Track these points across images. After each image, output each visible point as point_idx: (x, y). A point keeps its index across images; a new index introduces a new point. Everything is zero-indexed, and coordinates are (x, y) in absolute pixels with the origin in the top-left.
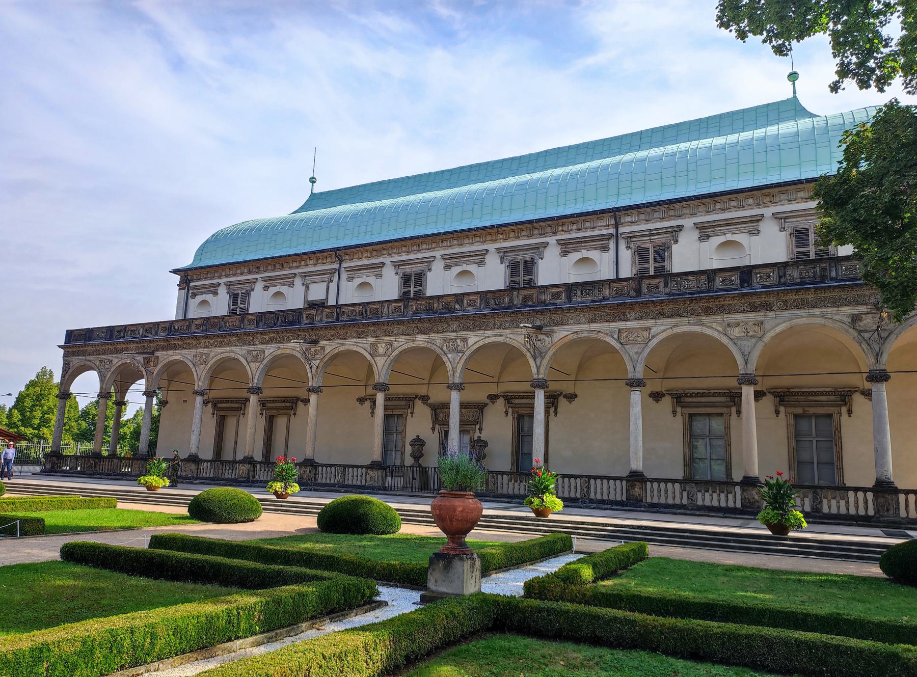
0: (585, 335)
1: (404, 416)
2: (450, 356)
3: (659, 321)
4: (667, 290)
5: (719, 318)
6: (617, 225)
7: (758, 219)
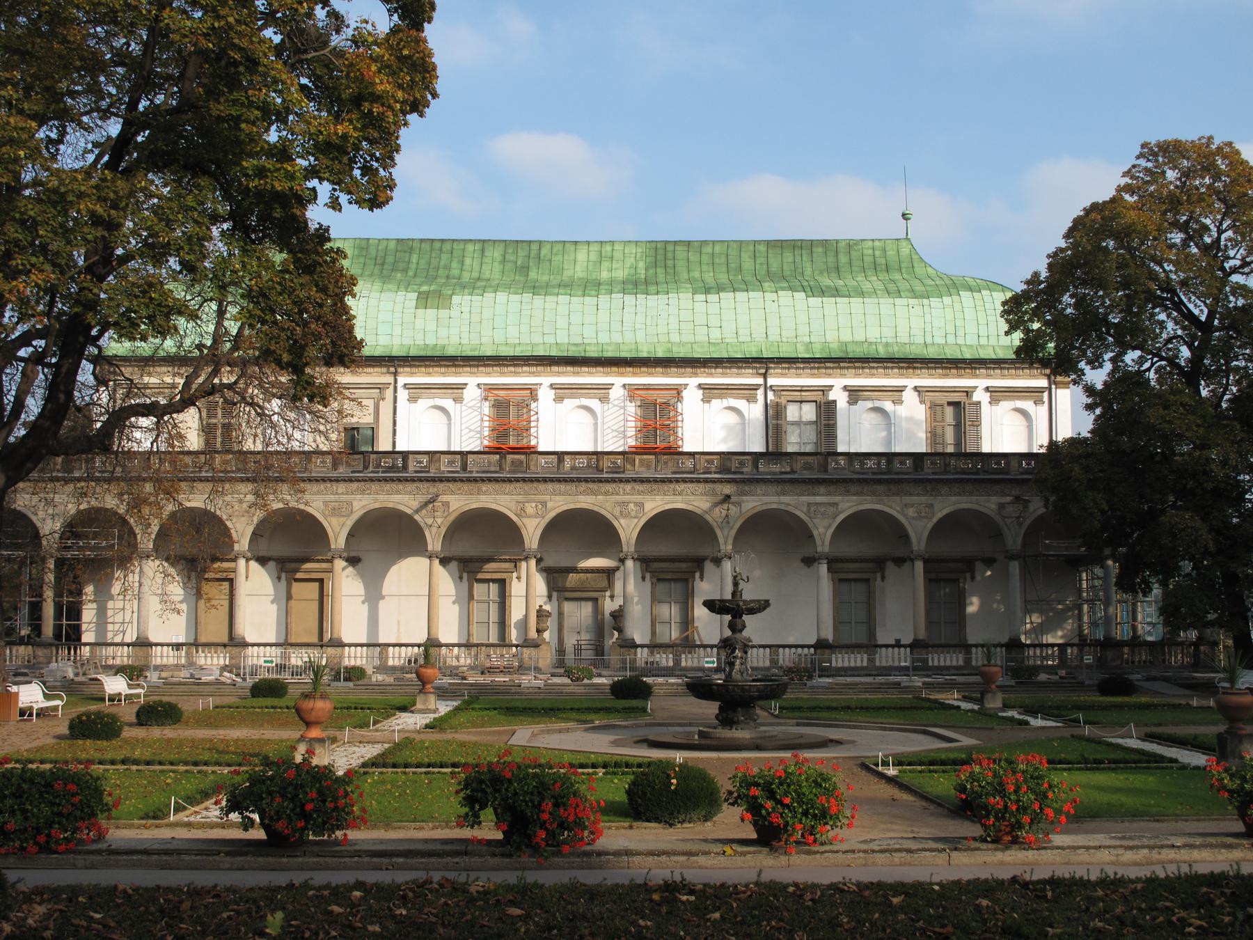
0: (774, 506)
1: (507, 581)
2: (622, 521)
3: (846, 498)
4: (852, 469)
5: (898, 498)
6: (765, 376)
7: (900, 390)
